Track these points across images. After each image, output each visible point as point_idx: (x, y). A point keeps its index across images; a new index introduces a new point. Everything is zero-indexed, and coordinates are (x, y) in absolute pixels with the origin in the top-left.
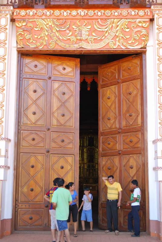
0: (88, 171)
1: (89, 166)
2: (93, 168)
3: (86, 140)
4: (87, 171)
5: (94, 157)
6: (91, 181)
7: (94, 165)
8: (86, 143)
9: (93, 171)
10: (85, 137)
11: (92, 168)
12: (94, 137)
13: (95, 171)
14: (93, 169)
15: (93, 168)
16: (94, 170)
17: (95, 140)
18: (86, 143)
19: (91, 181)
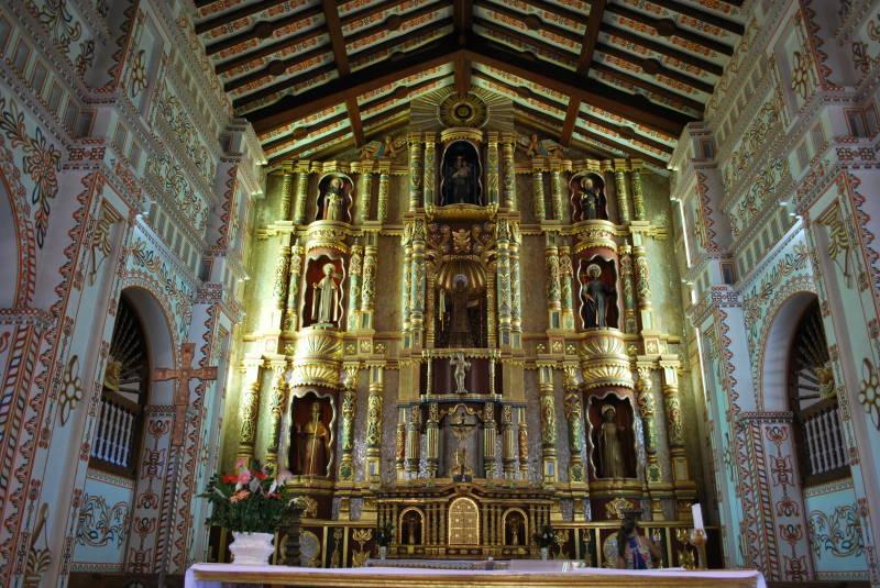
0: (433, 418)
1: (439, 375)
2: (484, 389)
3: (421, 171)
4: (421, 429)
5: (490, 295)
6: (463, 519)
7: (486, 361)
8: (420, 188)
9: (481, 424)
10: (414, 149)
11: (476, 396)
12: (484, 146)
13: (501, 428)
14: (480, 405)
15: (484, 389)
16: (489, 408)
17: (494, 164)
18: (420, 188)
19: (463, 519)
